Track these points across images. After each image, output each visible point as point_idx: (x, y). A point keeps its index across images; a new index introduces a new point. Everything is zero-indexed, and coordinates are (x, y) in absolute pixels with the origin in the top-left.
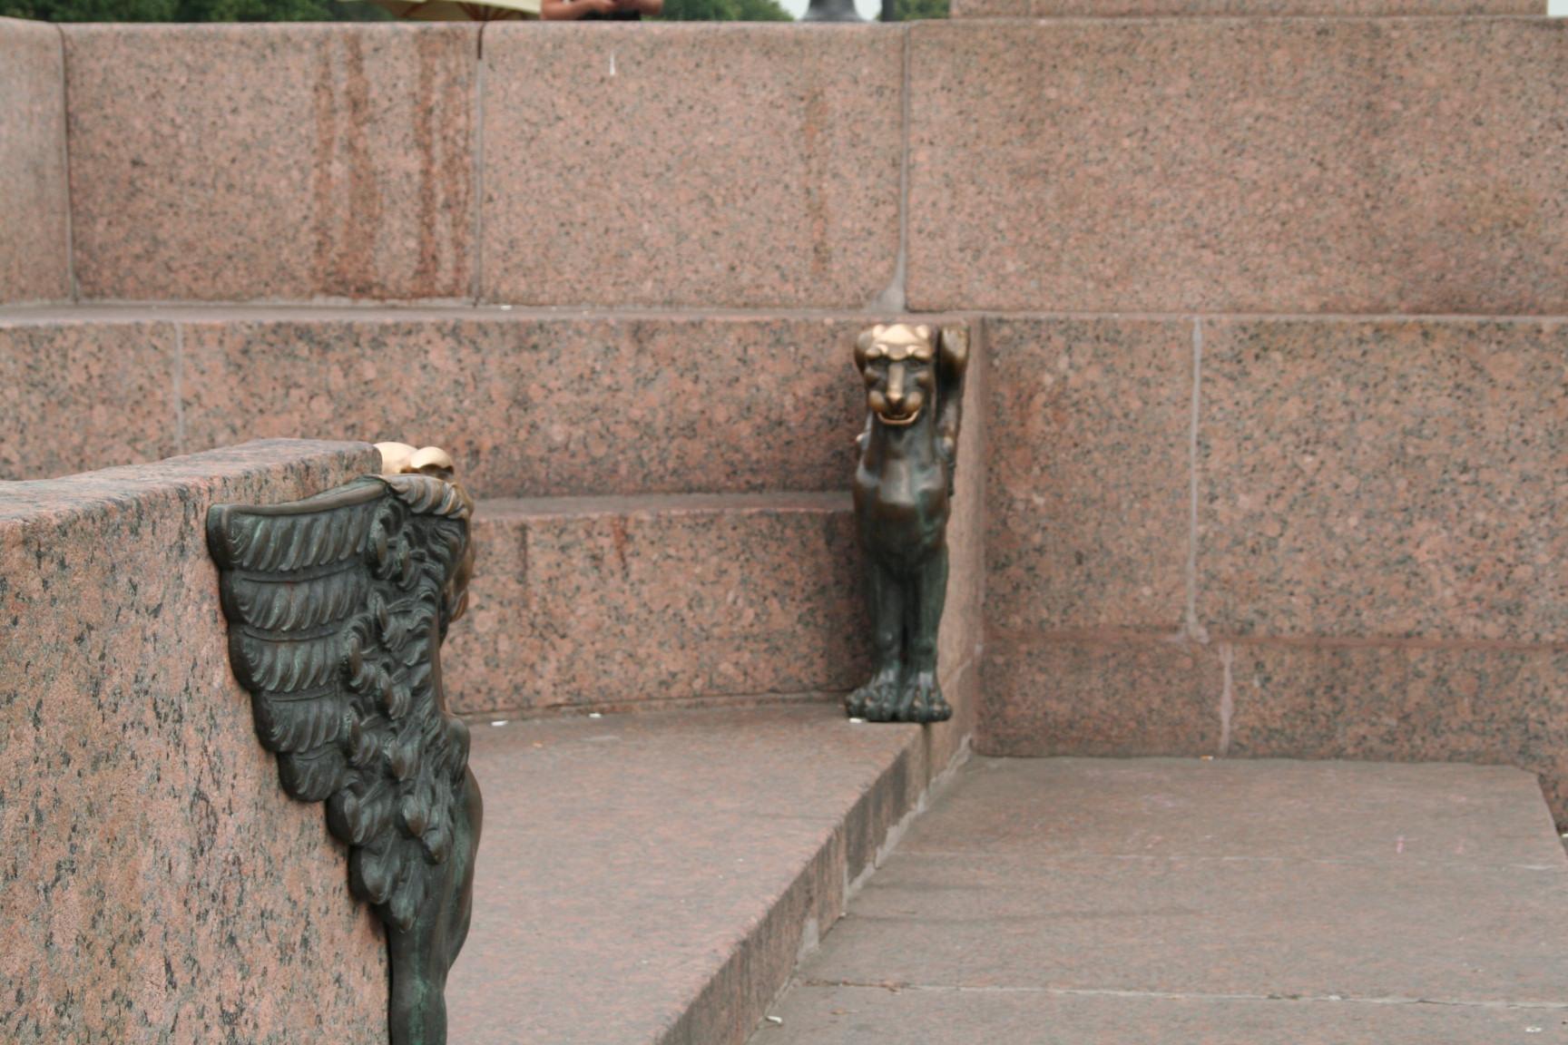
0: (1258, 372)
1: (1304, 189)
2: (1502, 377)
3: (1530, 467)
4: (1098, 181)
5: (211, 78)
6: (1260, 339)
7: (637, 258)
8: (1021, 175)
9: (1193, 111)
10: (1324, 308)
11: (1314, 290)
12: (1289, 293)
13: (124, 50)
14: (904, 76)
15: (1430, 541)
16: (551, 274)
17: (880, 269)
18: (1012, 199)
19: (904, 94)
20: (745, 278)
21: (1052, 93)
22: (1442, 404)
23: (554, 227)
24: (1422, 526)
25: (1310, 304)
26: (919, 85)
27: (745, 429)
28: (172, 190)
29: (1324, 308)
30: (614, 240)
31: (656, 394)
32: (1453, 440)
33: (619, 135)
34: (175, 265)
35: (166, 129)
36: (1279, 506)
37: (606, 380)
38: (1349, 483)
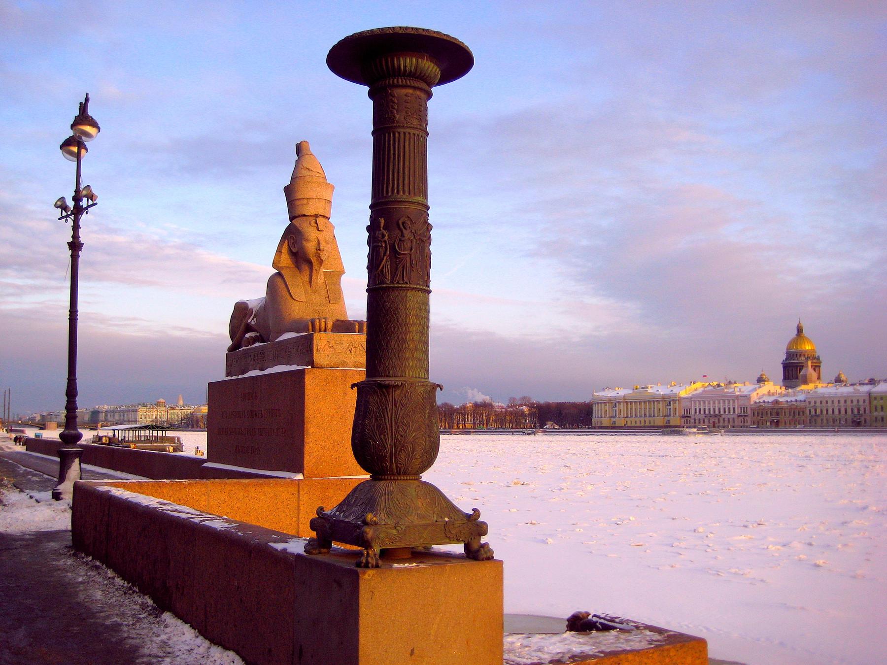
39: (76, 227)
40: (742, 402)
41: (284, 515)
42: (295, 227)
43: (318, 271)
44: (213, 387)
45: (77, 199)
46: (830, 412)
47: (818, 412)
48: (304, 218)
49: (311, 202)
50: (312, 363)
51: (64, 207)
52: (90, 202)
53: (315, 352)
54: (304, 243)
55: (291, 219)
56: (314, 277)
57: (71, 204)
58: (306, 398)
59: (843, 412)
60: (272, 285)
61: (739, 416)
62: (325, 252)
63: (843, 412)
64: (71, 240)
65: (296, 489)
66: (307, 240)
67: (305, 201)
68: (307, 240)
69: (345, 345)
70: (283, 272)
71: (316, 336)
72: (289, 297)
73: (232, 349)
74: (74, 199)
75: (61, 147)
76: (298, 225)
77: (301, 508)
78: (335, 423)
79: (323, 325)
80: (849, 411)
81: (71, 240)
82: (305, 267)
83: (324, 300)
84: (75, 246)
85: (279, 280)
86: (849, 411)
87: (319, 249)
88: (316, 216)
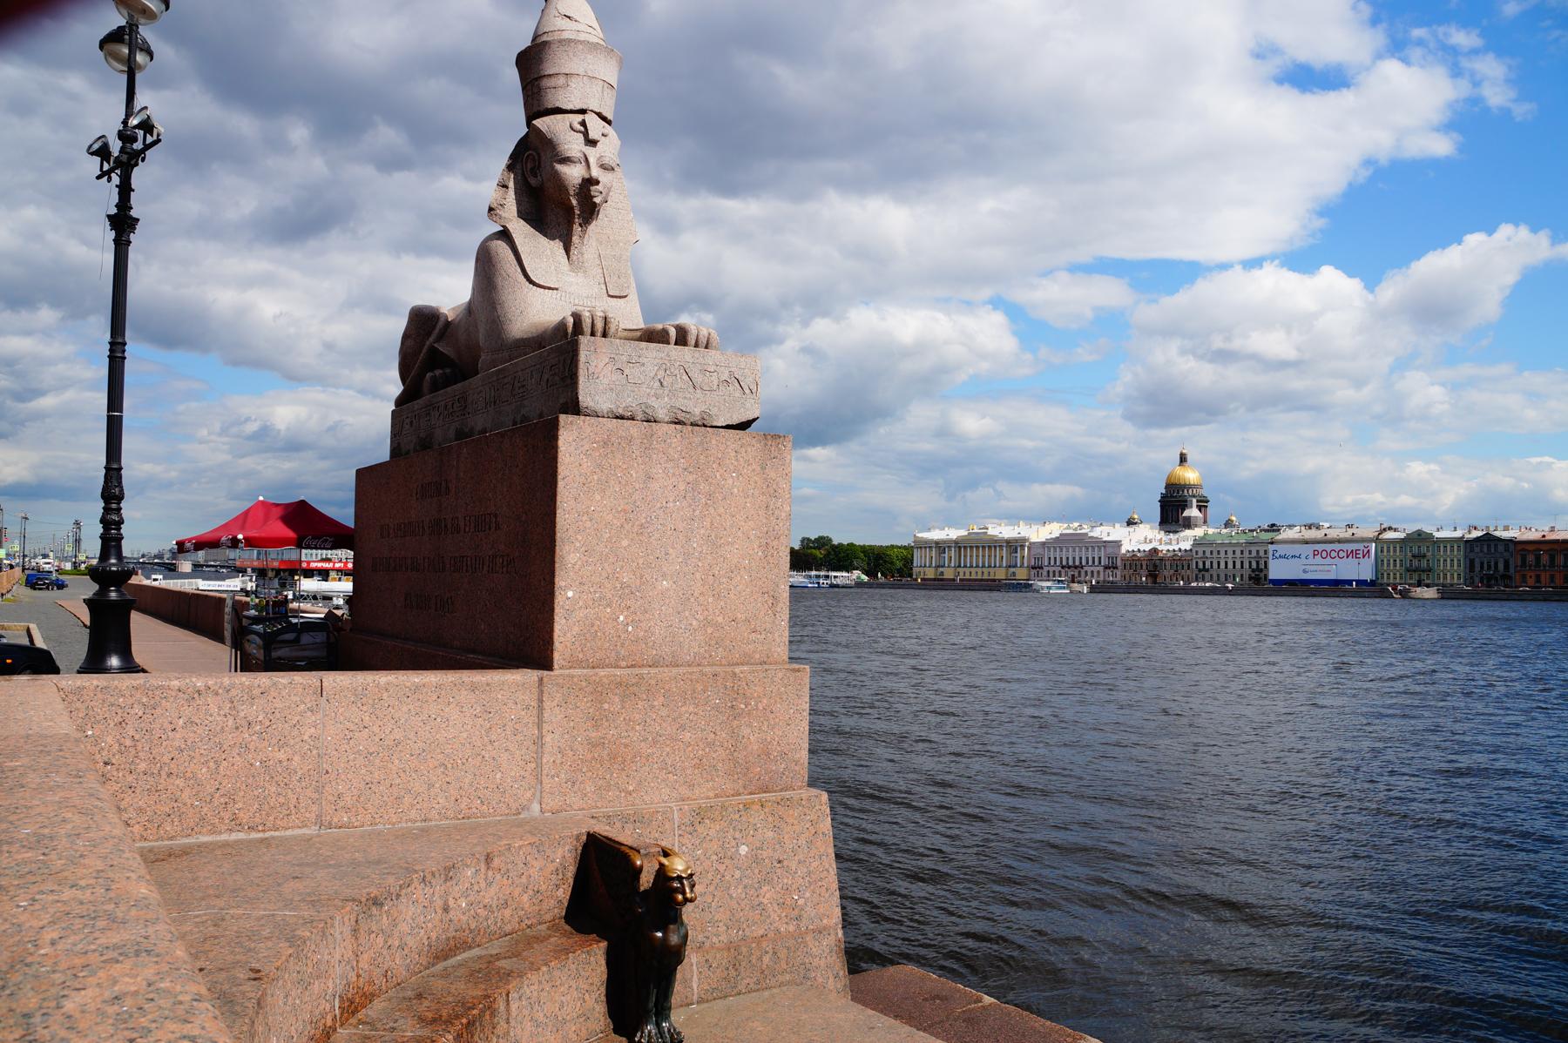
0: (700, 828)
1: (708, 744)
2: (790, 821)
3: (801, 857)
4: (626, 746)
5: (158, 711)
6: (700, 815)
7: (407, 800)
8: (593, 745)
9: (664, 712)
10: (716, 796)
11: (713, 789)
12: (704, 792)
13: (100, 696)
14: (541, 701)
15: (768, 894)
16: (361, 810)
17: (528, 794)
18: (589, 756)
19: (541, 709)
20: (463, 806)
21: (606, 706)
22: (770, 834)
23: (362, 785)
24: (765, 889)
25: (711, 794)
26: (547, 704)
27: (525, 898)
28: (130, 778)
29: (716, 796)
30: (395, 790)
31: (493, 890)
32: (774, 850)
33: (398, 735)
34: (132, 822)
35: (128, 742)
36: (711, 888)
37: (476, 888)
38: (738, 874)
39: (125, 190)
40: (1110, 550)
41: (505, 756)
42: (538, 131)
44: (367, 477)
45: (126, 136)
46: (1222, 565)
47: (1208, 565)
48: (559, 116)
49: (573, 83)
50: (574, 408)
51: (103, 152)
52: (149, 139)
54: (559, 167)
55: (529, 124)
56: (575, 239)
57: (115, 147)
58: (561, 484)
59: (1238, 565)
61: (1106, 568)
62: (599, 187)
63: (1238, 565)
64: (114, 211)
65: (535, 696)
67: (561, 81)
69: (651, 369)
71: (584, 340)
74: (121, 135)
75: (103, 43)
77: (548, 738)
78: (625, 543)
79: (599, 325)
80: (1246, 565)
81: (114, 211)
84: (123, 223)
86: (1246, 565)
88: (583, 112)
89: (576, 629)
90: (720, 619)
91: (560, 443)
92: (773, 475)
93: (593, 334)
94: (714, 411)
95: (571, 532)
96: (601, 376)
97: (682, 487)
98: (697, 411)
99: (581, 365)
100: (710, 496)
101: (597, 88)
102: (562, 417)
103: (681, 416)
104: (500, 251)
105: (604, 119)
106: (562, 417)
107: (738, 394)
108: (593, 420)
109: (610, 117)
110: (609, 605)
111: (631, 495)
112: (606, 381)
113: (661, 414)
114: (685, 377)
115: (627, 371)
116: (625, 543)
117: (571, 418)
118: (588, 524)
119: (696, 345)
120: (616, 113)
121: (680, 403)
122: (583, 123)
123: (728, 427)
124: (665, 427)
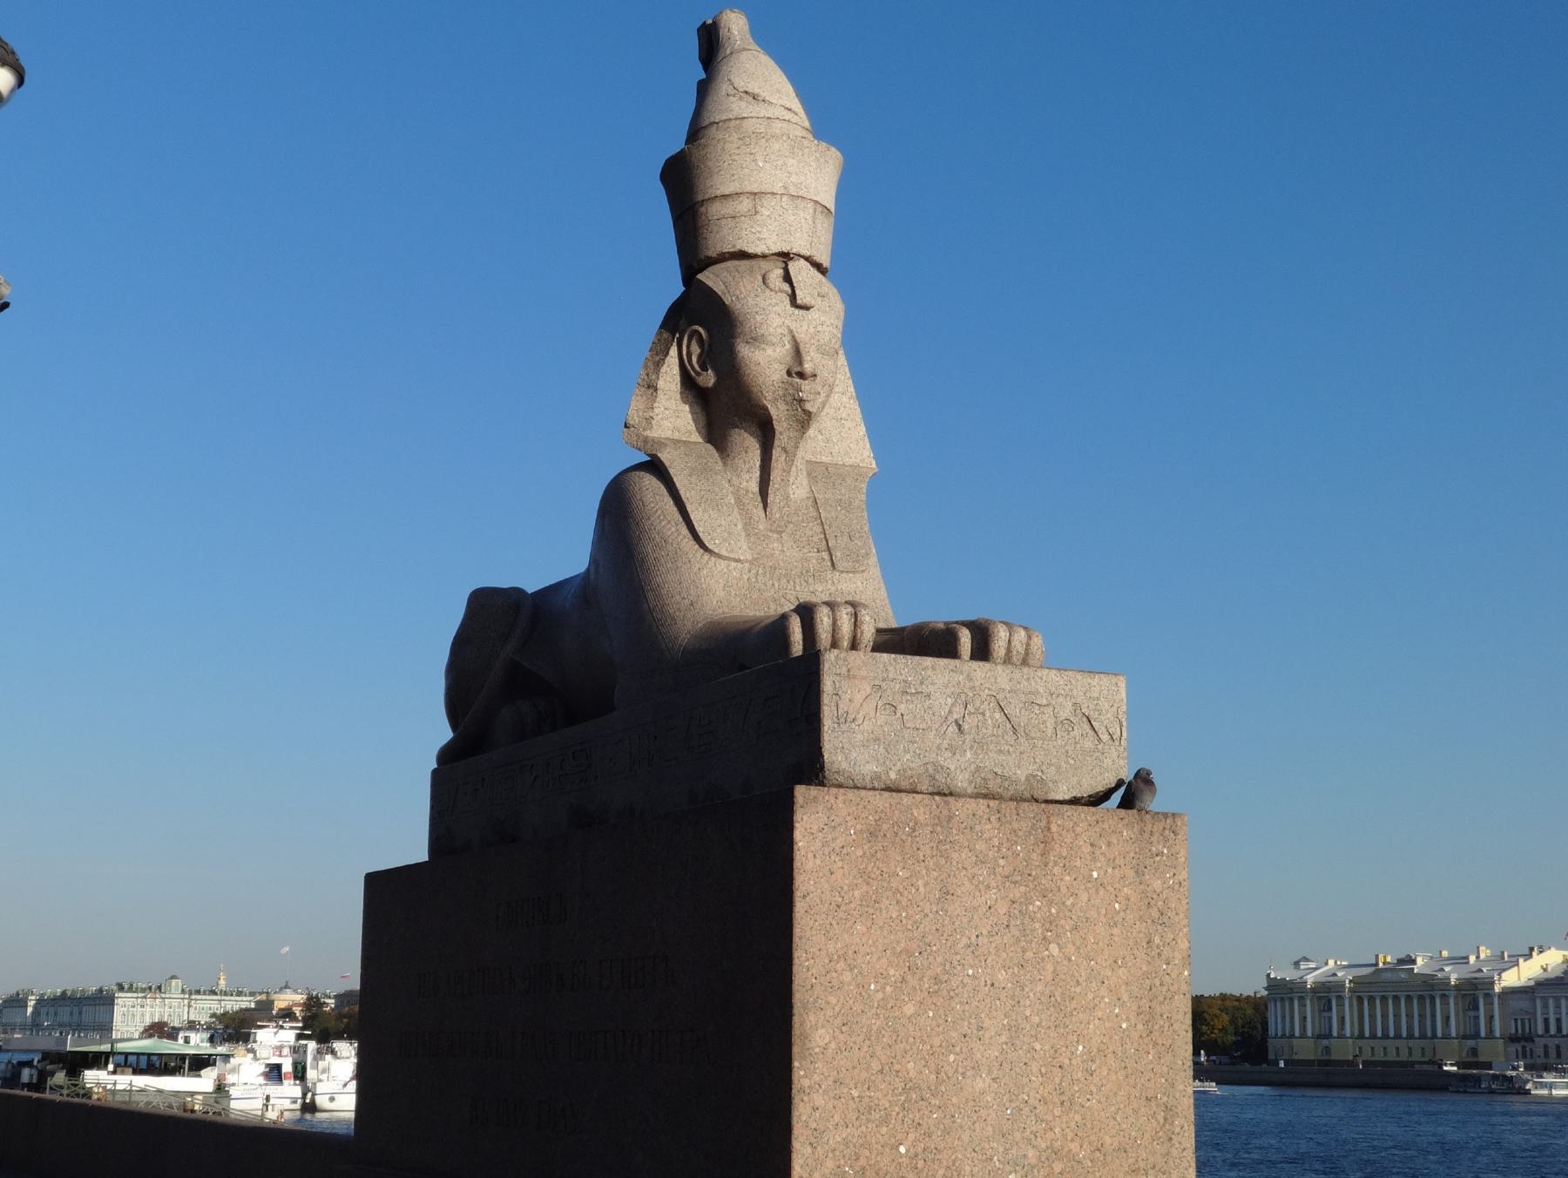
43: (790, 454)
48: (744, 264)
49: (767, 208)
53: (828, 723)
55: (689, 276)
56: (776, 475)
60: (617, 513)
62: (817, 385)
66: (756, 340)
67: (745, 205)
68: (756, 340)
69: (942, 703)
70: (664, 456)
72: (688, 543)
73: (447, 756)
76: (718, 288)
78: (909, 1009)
82: (747, 445)
83: (814, 559)
85: (649, 482)
87: (797, 372)
88: (785, 256)
89: (830, 1164)
90: (1074, 1147)
91: (798, 834)
92: (1157, 884)
93: (835, 644)
94: (1051, 772)
95: (818, 990)
96: (867, 712)
97: (1002, 908)
98: (1021, 774)
99: (826, 699)
100: (1050, 923)
101: (806, 213)
102: (801, 792)
103: (993, 785)
104: (648, 498)
105: (818, 266)
106: (801, 792)
107: (1089, 744)
108: (851, 794)
109: (826, 262)
110: (885, 1121)
111: (917, 924)
112: (867, 726)
113: (962, 781)
114: (998, 715)
115: (902, 708)
116: (909, 1009)
117: (814, 791)
118: (847, 977)
119: (1008, 660)
120: (835, 254)
121: (990, 761)
122: (787, 278)
123: (1075, 801)
124: (971, 805)
